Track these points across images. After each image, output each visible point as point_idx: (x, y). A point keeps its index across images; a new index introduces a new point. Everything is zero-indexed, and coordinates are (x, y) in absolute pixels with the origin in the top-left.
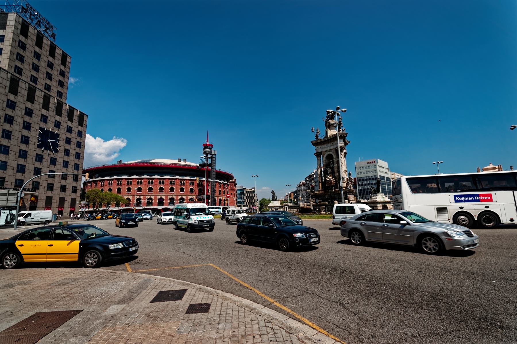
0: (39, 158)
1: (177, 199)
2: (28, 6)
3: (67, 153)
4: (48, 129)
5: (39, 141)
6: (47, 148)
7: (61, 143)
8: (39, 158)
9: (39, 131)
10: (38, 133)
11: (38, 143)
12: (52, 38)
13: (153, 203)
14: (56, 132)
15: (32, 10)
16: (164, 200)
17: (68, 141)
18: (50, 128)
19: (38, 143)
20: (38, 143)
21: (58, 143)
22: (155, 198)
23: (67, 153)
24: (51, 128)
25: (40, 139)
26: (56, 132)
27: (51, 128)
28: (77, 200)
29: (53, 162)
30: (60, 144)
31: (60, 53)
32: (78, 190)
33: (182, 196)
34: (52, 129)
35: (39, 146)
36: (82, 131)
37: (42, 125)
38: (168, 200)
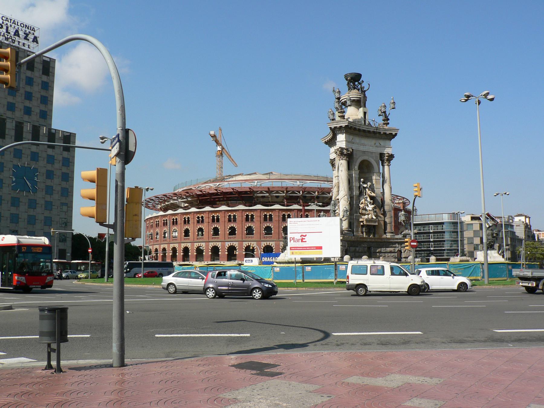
0: (15, 202)
1: (241, 247)
2: (3, 18)
3: (49, 190)
4: (23, 165)
5: (13, 182)
6: (25, 188)
7: (40, 179)
8: (15, 202)
9: (13, 170)
10: (11, 172)
11: (12, 185)
12: (35, 43)
13: (220, 256)
14: (33, 166)
15: (8, 21)
16: (220, 251)
17: (50, 175)
18: (25, 164)
19: (12, 184)
20: (12, 185)
21: (36, 179)
22: (223, 246)
23: (49, 190)
24: (26, 163)
25: (14, 179)
26: (33, 166)
27: (26, 163)
28: (67, 251)
29: (32, 204)
30: (39, 181)
31: (41, 61)
32: (67, 239)
33: (268, 243)
34: (27, 164)
35: (14, 189)
36: (69, 157)
37: (16, 162)
38: (281, 250)
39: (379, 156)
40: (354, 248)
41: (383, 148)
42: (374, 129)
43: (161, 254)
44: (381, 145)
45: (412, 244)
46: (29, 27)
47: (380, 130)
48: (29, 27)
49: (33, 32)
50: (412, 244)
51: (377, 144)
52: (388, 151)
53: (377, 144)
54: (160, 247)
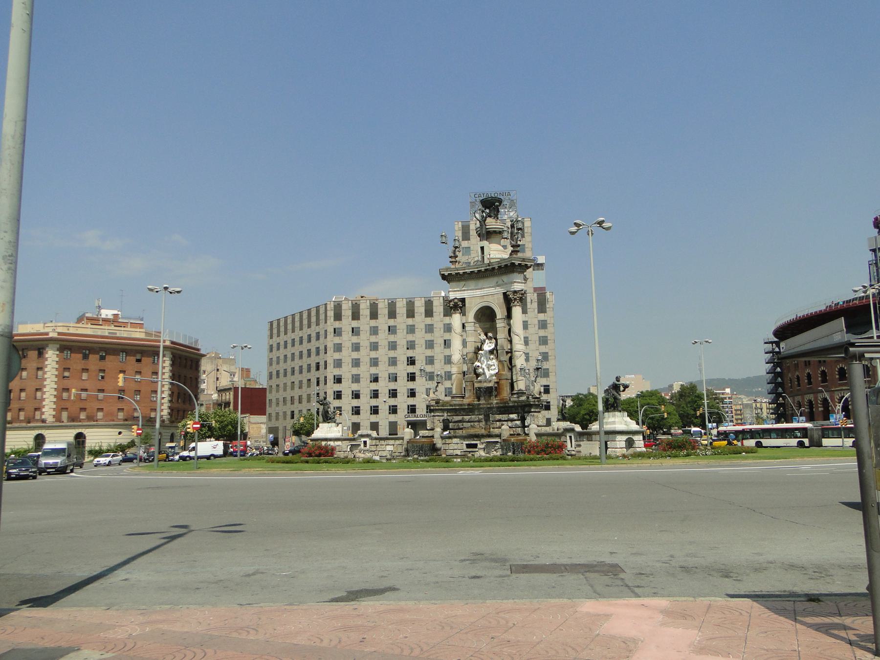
39: (502, 297)
40: (462, 417)
41: (510, 285)
42: (486, 267)
43: (821, 409)
44: (503, 282)
45: (194, 426)
46: (504, 194)
47: (493, 265)
48: (504, 194)
49: (509, 196)
50: (194, 426)
51: (500, 282)
52: (517, 287)
53: (500, 282)
54: (803, 399)
